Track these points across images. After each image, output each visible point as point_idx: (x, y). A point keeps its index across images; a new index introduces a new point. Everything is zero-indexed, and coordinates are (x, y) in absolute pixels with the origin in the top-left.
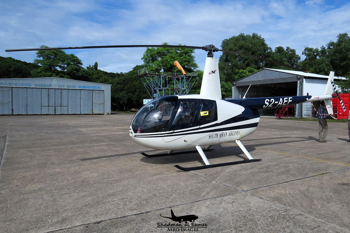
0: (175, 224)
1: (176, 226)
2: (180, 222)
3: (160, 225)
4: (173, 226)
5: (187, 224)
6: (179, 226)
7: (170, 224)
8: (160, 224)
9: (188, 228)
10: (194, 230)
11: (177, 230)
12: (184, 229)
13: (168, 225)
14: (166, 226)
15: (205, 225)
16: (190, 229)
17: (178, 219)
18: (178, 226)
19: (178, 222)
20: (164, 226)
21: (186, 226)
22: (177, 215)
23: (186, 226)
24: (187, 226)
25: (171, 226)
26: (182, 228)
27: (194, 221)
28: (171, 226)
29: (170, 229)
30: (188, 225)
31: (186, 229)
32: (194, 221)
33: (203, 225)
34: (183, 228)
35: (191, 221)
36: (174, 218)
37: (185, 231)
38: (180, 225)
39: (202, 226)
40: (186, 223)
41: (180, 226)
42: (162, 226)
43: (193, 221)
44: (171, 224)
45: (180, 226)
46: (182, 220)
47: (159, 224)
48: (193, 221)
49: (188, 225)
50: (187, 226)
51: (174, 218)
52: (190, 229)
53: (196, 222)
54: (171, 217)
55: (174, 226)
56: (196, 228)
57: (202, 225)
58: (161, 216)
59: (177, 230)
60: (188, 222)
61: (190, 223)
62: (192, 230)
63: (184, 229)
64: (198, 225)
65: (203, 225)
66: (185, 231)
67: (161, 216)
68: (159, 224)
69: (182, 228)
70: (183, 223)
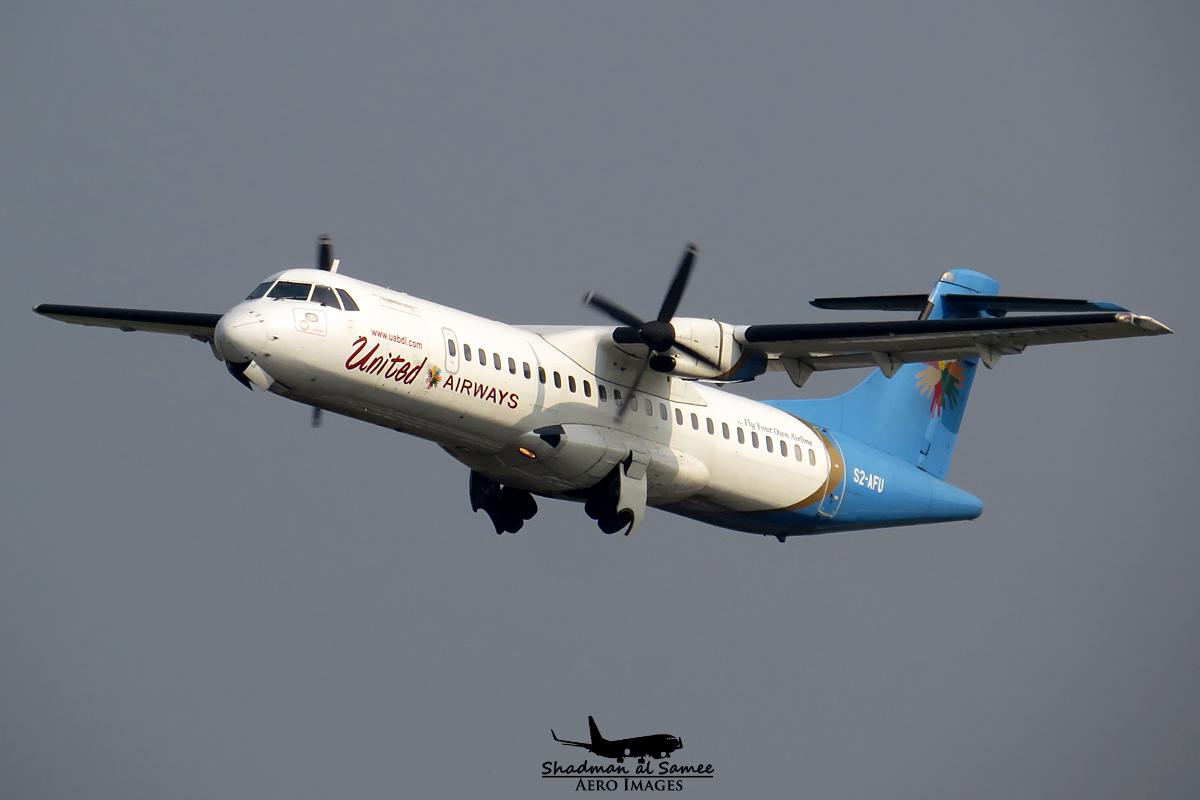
0: (601, 768)
1: (606, 774)
2: (620, 760)
3: (551, 770)
4: (595, 774)
5: (645, 766)
6: (616, 774)
7: (584, 766)
8: (552, 767)
9: (647, 779)
10: (666, 788)
11: (612, 785)
12: (633, 783)
13: (578, 771)
14: (572, 774)
15: (707, 771)
16: (653, 781)
18: (612, 774)
19: (613, 761)
20: (565, 774)
21: (641, 774)
22: (609, 734)
24: (646, 774)
25: (589, 774)
26: (626, 781)
27: (668, 756)
28: (589, 774)
29: (585, 782)
31: (640, 784)
32: (668, 756)
33: (699, 770)
34: (630, 781)
35: (657, 756)
36: (599, 745)
37: (637, 788)
38: (619, 770)
39: (697, 774)
40: (642, 761)
41: (622, 774)
42: (559, 773)
43: (663, 754)
44: (587, 768)
45: (622, 774)
46: (627, 752)
47: (547, 766)
50: (646, 774)
51: (599, 745)
52: (653, 781)
53: (677, 758)
54: (590, 742)
55: (601, 773)
56: (677, 779)
58: (555, 739)
59: (612, 785)
60: (647, 758)
61: (654, 764)
62: (660, 785)
63: (633, 783)
64: (682, 769)
65: (699, 770)
66: (637, 788)
67: (555, 739)
68: (547, 766)
69: (626, 781)
70: (631, 763)
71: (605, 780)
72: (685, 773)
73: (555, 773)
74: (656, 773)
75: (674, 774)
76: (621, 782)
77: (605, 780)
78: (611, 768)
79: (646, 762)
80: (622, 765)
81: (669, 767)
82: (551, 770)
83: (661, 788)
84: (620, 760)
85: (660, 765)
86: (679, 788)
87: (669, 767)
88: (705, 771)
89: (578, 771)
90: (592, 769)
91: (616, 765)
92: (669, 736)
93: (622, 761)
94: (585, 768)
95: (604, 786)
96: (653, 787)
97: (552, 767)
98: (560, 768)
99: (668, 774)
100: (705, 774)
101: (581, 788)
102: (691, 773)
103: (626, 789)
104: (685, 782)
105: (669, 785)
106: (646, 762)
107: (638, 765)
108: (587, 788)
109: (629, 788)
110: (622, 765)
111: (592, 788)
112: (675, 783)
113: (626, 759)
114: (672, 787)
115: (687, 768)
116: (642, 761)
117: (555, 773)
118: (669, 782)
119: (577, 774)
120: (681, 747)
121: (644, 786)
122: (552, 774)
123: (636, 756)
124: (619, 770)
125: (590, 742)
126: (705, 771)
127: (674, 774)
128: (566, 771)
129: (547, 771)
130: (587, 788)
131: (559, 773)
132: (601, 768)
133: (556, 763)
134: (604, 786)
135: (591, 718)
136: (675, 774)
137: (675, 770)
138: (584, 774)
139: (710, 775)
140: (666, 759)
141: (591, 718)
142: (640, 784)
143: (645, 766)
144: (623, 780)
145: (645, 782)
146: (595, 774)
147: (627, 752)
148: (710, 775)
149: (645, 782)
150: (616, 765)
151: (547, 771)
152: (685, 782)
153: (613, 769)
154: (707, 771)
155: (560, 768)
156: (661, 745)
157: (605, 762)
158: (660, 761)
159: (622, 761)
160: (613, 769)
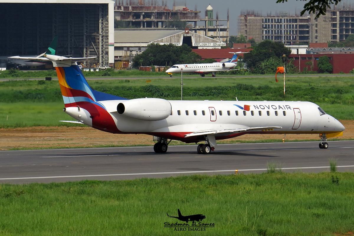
0: (182, 224)
2: (187, 222)
5: (194, 224)
7: (177, 224)
8: (167, 224)
10: (201, 230)
12: (191, 229)
13: (175, 225)
14: (173, 226)
15: (213, 225)
17: (185, 219)
18: (185, 226)
19: (185, 222)
21: (193, 226)
22: (184, 214)
23: (193, 226)
25: (177, 226)
27: (201, 221)
28: (177, 226)
29: (177, 228)
31: (193, 229)
32: (201, 221)
33: (210, 225)
34: (190, 228)
35: (198, 221)
36: (181, 218)
37: (192, 230)
38: (187, 225)
41: (188, 226)
42: (169, 226)
43: (200, 220)
44: (178, 224)
45: (188, 226)
46: (189, 219)
47: (165, 223)
49: (195, 225)
50: (195, 226)
51: (181, 218)
53: (204, 221)
56: (204, 228)
58: (168, 216)
60: (195, 221)
62: (199, 230)
64: (205, 225)
65: (210, 225)
70: (190, 223)
71: (183, 228)
76: (187, 229)
81: (201, 224)
84: (187, 222)
87: (201, 224)
89: (175, 225)
90: (179, 225)
100: (212, 226)
103: (189, 230)
108: (177, 230)
109: (190, 230)
110: (187, 223)
113: (189, 222)
119: (174, 226)
122: (167, 226)
123: (192, 221)
124: (187, 225)
128: (171, 225)
130: (177, 230)
131: (169, 226)
134: (182, 230)
136: (203, 226)
140: (201, 222)
142: (193, 229)
143: (194, 224)
144: (188, 228)
154: (213, 225)
156: (199, 217)
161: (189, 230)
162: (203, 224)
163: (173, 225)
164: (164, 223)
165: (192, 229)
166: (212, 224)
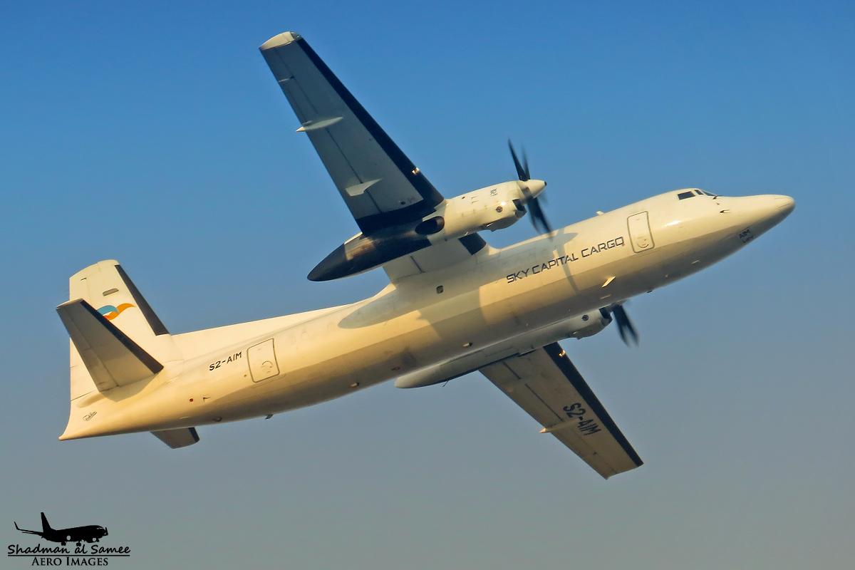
0: (50, 549)
1: (53, 554)
2: (64, 544)
3: (14, 551)
4: (45, 553)
5: (81, 548)
6: (60, 553)
7: (38, 548)
8: (15, 549)
10: (97, 563)
12: (73, 560)
13: (33, 551)
14: (29, 554)
15: (125, 551)
16: (87, 559)
17: (59, 536)
18: (58, 553)
19: (59, 544)
20: (24, 554)
21: (78, 554)
22: (56, 526)
23: (78, 554)
24: (82, 554)
25: (41, 553)
27: (98, 541)
28: (41, 553)
29: (39, 559)
30: (83, 550)
31: (78, 561)
32: (98, 541)
33: (119, 551)
34: (70, 558)
35: (90, 541)
36: (48, 533)
37: (75, 564)
38: (63, 551)
39: (118, 554)
40: (79, 544)
41: (65, 553)
42: (20, 553)
43: (94, 539)
44: (40, 549)
45: (65, 553)
46: (69, 538)
47: (12, 548)
48: (94, 539)
49: (83, 550)
50: (82, 554)
51: (48, 533)
52: (87, 559)
53: (104, 542)
54: (42, 531)
55: (50, 553)
56: (103, 558)
57: (117, 550)
58: (17, 528)
60: (83, 542)
61: (88, 546)
62: (92, 563)
63: (73, 560)
65: (119, 551)
66: (75, 564)
67: (17, 528)
68: (12, 548)
70: (71, 546)
71: (53, 558)
72: (110, 553)
73: (17, 553)
74: (89, 553)
75: (101, 554)
77: (53, 558)
78: (57, 549)
79: (82, 545)
80: (65, 547)
81: (98, 549)
82: (14, 551)
83: (92, 564)
84: (64, 544)
85: (92, 548)
86: (105, 564)
87: (98, 549)
88: (124, 551)
90: (43, 550)
91: (61, 547)
92: (98, 527)
93: (65, 544)
94: (38, 550)
95: (52, 562)
96: (87, 563)
97: (15, 549)
98: (21, 549)
99: (98, 553)
100: (124, 554)
101: (35, 564)
102: (114, 553)
103: (68, 564)
104: (110, 559)
105: (99, 561)
106: (82, 545)
107: (76, 547)
108: (40, 563)
109: (70, 564)
110: (63, 547)
111: (43, 563)
112: (103, 560)
113: (68, 543)
114: (100, 563)
115: (111, 549)
116: (79, 544)
117: (17, 553)
118: (98, 559)
119: (32, 554)
120: (107, 534)
121: (80, 563)
122: (15, 554)
123: (75, 541)
124: (63, 551)
125: (42, 531)
126: (124, 551)
127: (101, 554)
128: (25, 551)
129: (95, 551)
130: (40, 563)
131: (20, 553)
132: (50, 549)
133: (18, 546)
134: (52, 562)
135: (42, 514)
137: (103, 550)
138: (38, 553)
139: (128, 554)
140: (96, 543)
141: (42, 514)
143: (81, 548)
144: (66, 558)
145: (81, 559)
146: (45, 553)
147: (69, 538)
148: (128, 554)
149: (81, 559)
150: (61, 547)
151: (95, 551)
152: (110, 559)
153: (58, 550)
154: (125, 551)
155: (21, 549)
156: (92, 533)
157: (53, 545)
158: (92, 544)
159: (65, 544)
160: (58, 550)
161: (68, 564)
162: (102, 549)
163: (29, 551)
164: (9, 547)
165: (75, 561)
166: (123, 550)
